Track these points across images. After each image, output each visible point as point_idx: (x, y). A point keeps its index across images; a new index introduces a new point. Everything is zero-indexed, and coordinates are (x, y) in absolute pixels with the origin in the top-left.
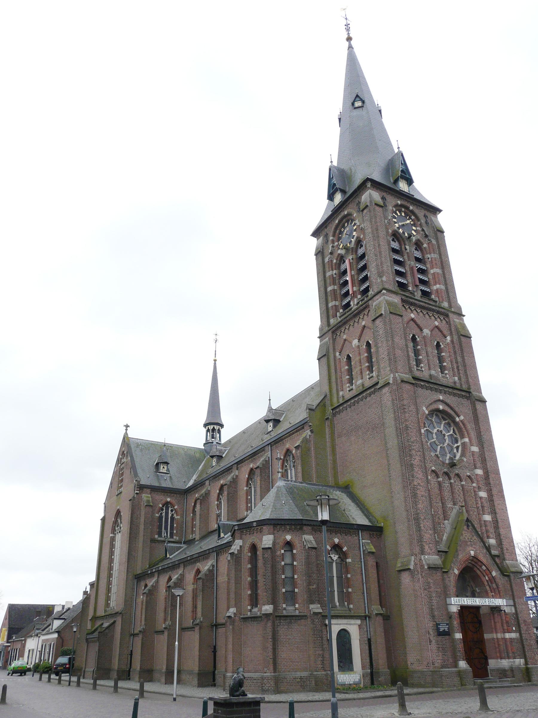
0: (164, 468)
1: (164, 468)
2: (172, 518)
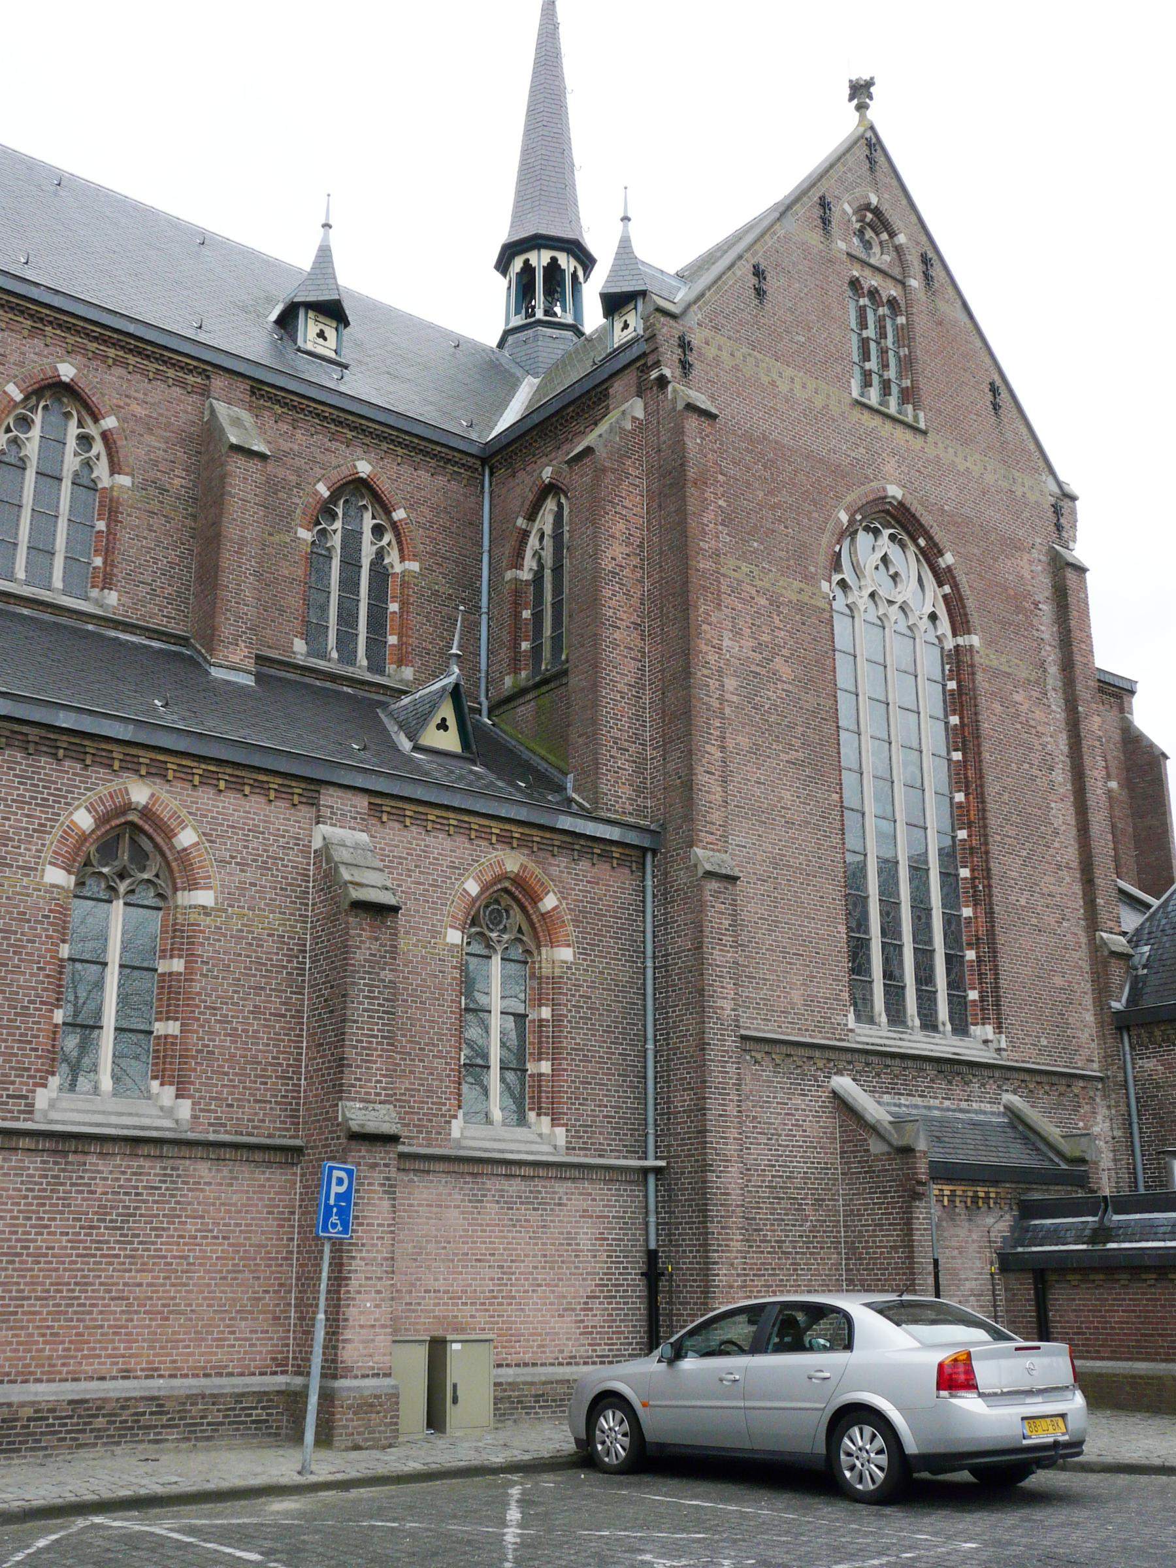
0: (321, 335)
1: (321, 335)
2: (380, 573)
